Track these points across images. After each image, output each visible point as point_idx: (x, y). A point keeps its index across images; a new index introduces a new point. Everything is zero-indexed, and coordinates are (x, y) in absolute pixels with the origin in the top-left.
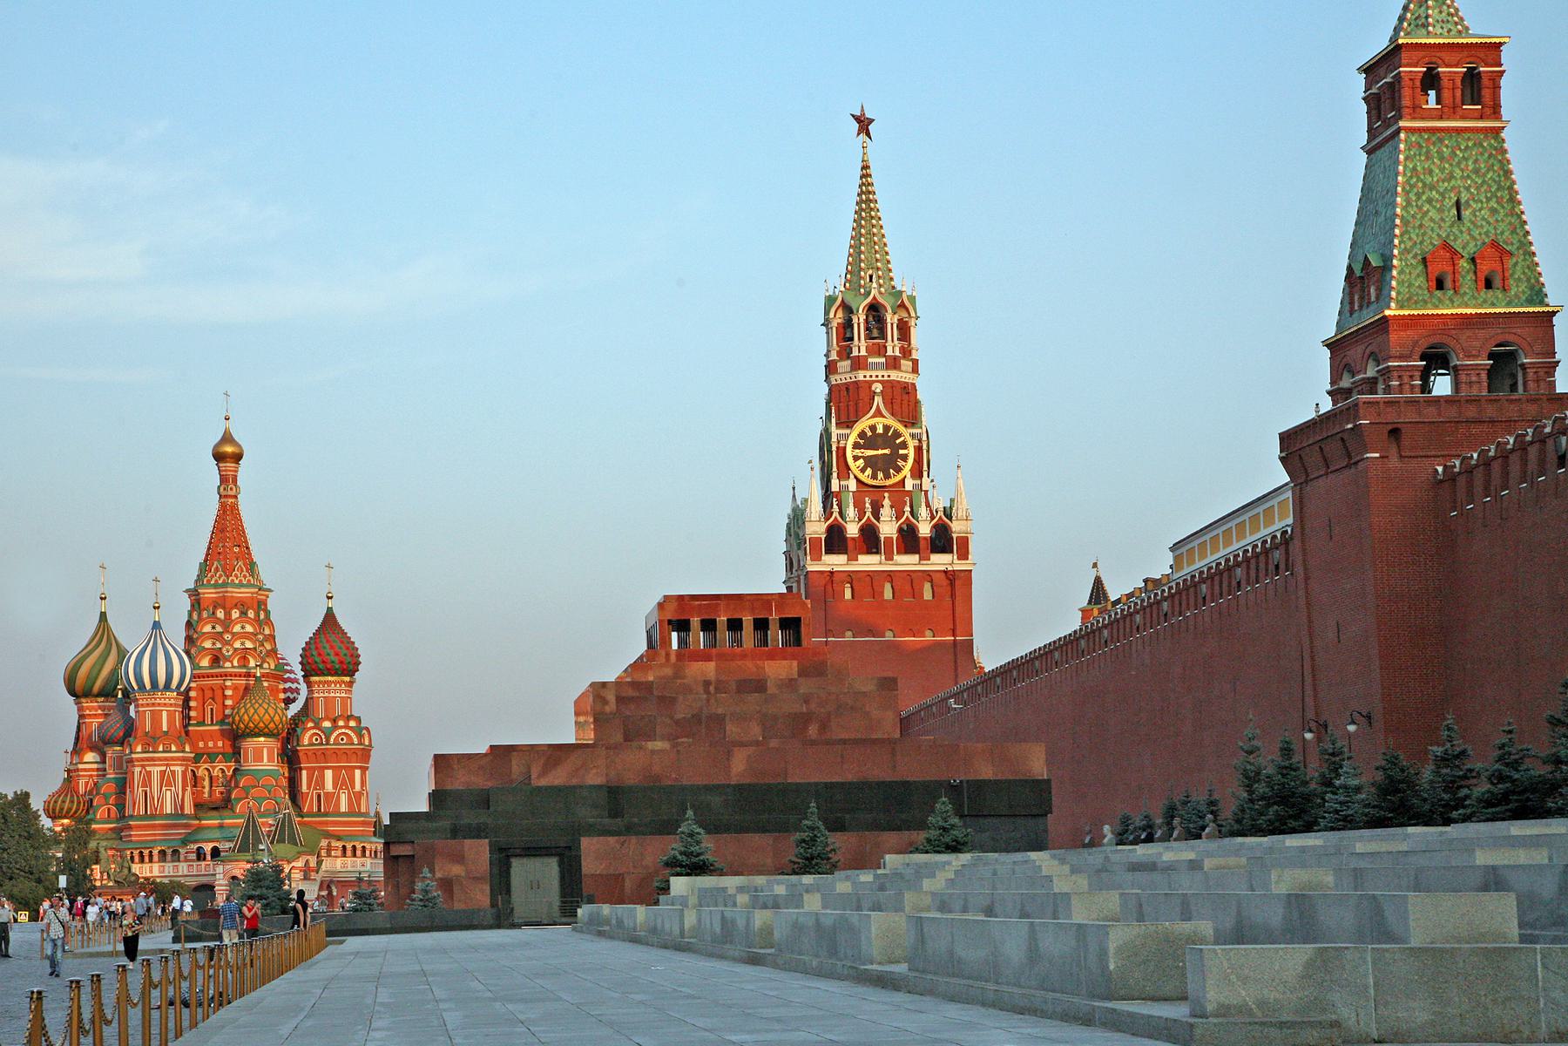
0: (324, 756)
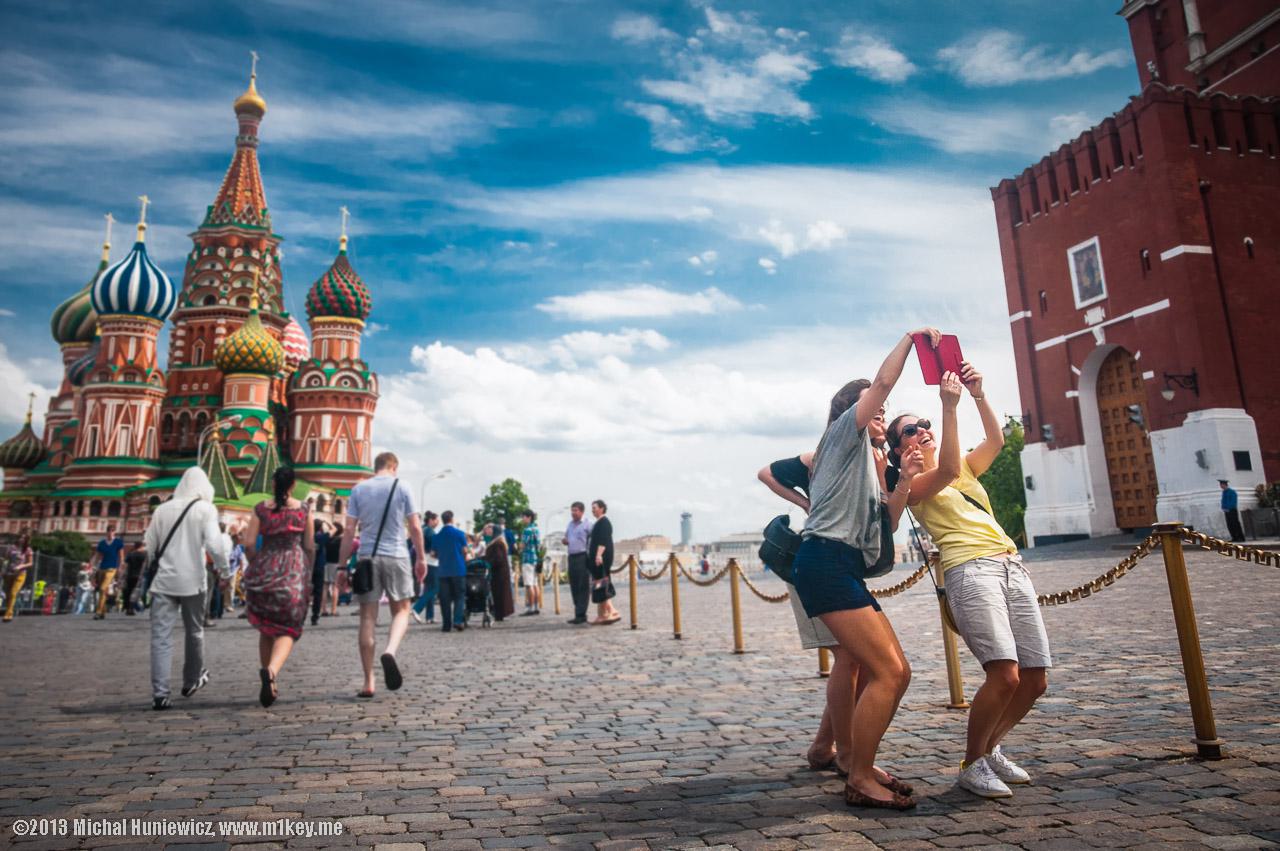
0: (320, 398)
